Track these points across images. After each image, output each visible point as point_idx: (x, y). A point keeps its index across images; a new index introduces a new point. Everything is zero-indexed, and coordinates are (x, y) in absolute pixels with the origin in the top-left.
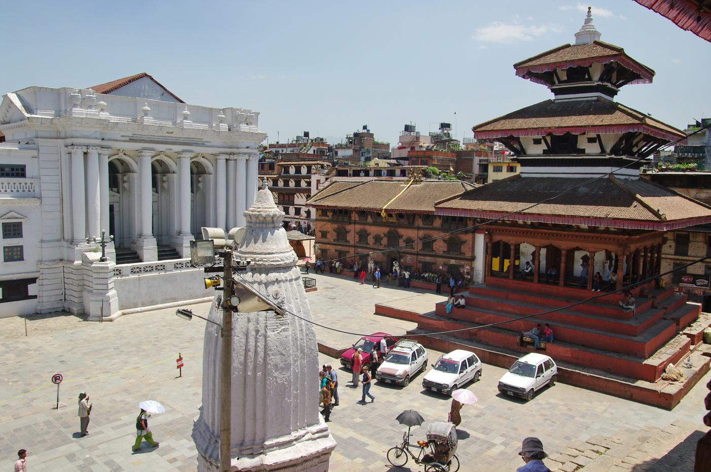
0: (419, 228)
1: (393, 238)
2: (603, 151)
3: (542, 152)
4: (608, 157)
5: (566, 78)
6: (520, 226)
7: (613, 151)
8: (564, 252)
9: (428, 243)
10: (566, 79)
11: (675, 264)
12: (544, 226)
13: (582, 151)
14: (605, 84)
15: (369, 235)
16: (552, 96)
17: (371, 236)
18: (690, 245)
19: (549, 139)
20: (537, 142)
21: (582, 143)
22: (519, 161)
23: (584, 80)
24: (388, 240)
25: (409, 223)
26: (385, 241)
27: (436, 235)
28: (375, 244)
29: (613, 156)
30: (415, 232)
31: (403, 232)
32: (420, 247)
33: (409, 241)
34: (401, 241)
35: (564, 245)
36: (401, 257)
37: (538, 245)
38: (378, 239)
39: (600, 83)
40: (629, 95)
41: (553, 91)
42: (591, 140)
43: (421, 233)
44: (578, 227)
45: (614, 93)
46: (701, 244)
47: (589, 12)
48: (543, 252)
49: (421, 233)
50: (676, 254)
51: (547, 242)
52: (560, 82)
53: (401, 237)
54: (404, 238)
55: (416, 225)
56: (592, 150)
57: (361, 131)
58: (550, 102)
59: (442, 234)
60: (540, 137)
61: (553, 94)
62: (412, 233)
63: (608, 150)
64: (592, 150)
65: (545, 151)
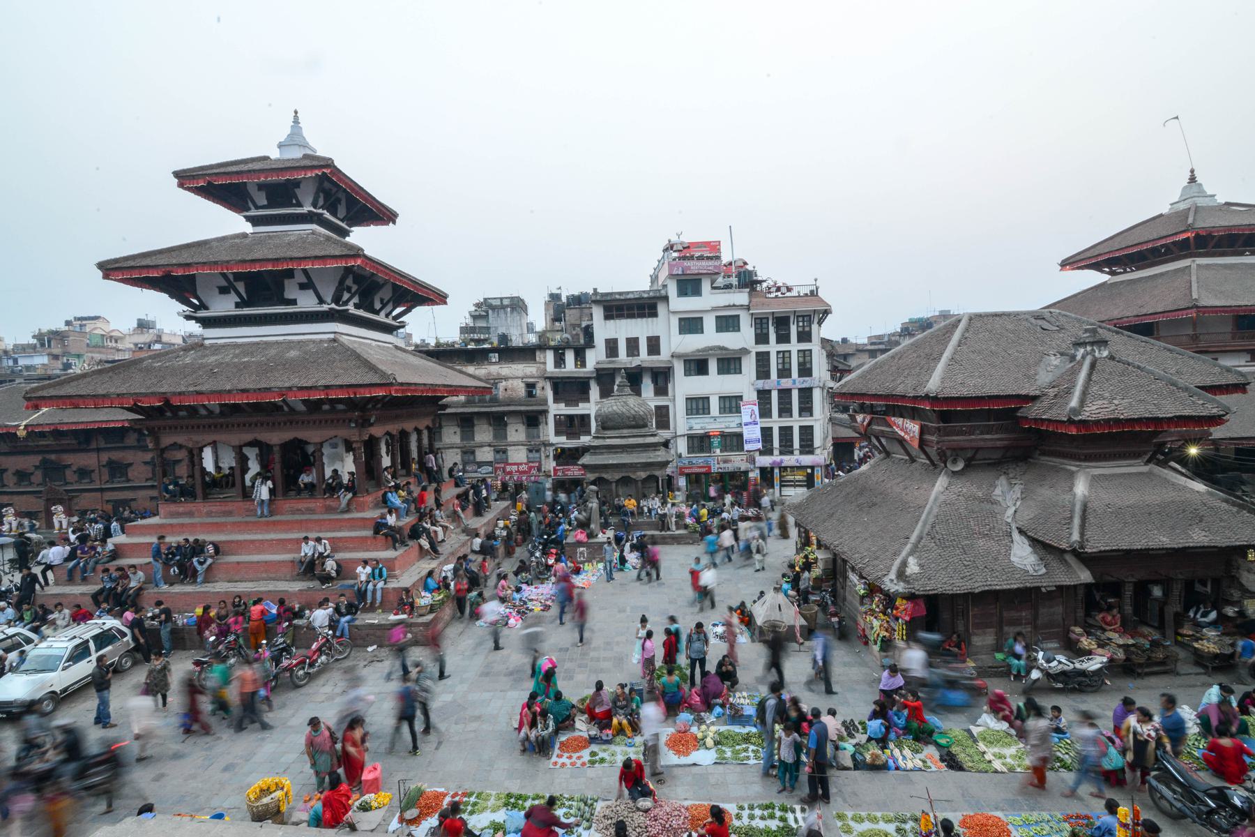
0: (98, 450)
1: (53, 470)
2: (321, 301)
3: (233, 306)
4: (325, 307)
5: (265, 203)
6: (202, 417)
7: (337, 300)
8: (276, 449)
9: (117, 469)
10: (265, 203)
11: (464, 453)
12: (236, 408)
13: (293, 302)
14: (320, 211)
15: (6, 470)
16: (248, 228)
17: (9, 473)
18: (476, 429)
19: (241, 287)
20: (223, 291)
21: (291, 291)
22: (198, 320)
23: (291, 205)
24: (45, 476)
25: (79, 443)
26: (38, 477)
27: (128, 456)
28: (18, 484)
29: (333, 306)
30: (94, 455)
31: (69, 459)
32: (106, 477)
33: (83, 473)
34: (68, 472)
35: (276, 438)
36: (70, 500)
37: (237, 443)
38: (22, 476)
39: (312, 209)
40: (364, 238)
41: (248, 219)
42: (303, 287)
43: (105, 457)
44: (292, 410)
45: (345, 233)
46: (486, 426)
47: (296, 121)
48: (251, 453)
49: (105, 457)
50: (462, 439)
51: (248, 437)
52: (257, 207)
53: (69, 466)
54: (74, 468)
55: (93, 446)
56: (307, 302)
57: (63, 328)
58: (245, 235)
59: (140, 454)
60: (224, 283)
61: (249, 224)
62: (88, 460)
63: (329, 300)
64: (307, 302)
65: (237, 305)
